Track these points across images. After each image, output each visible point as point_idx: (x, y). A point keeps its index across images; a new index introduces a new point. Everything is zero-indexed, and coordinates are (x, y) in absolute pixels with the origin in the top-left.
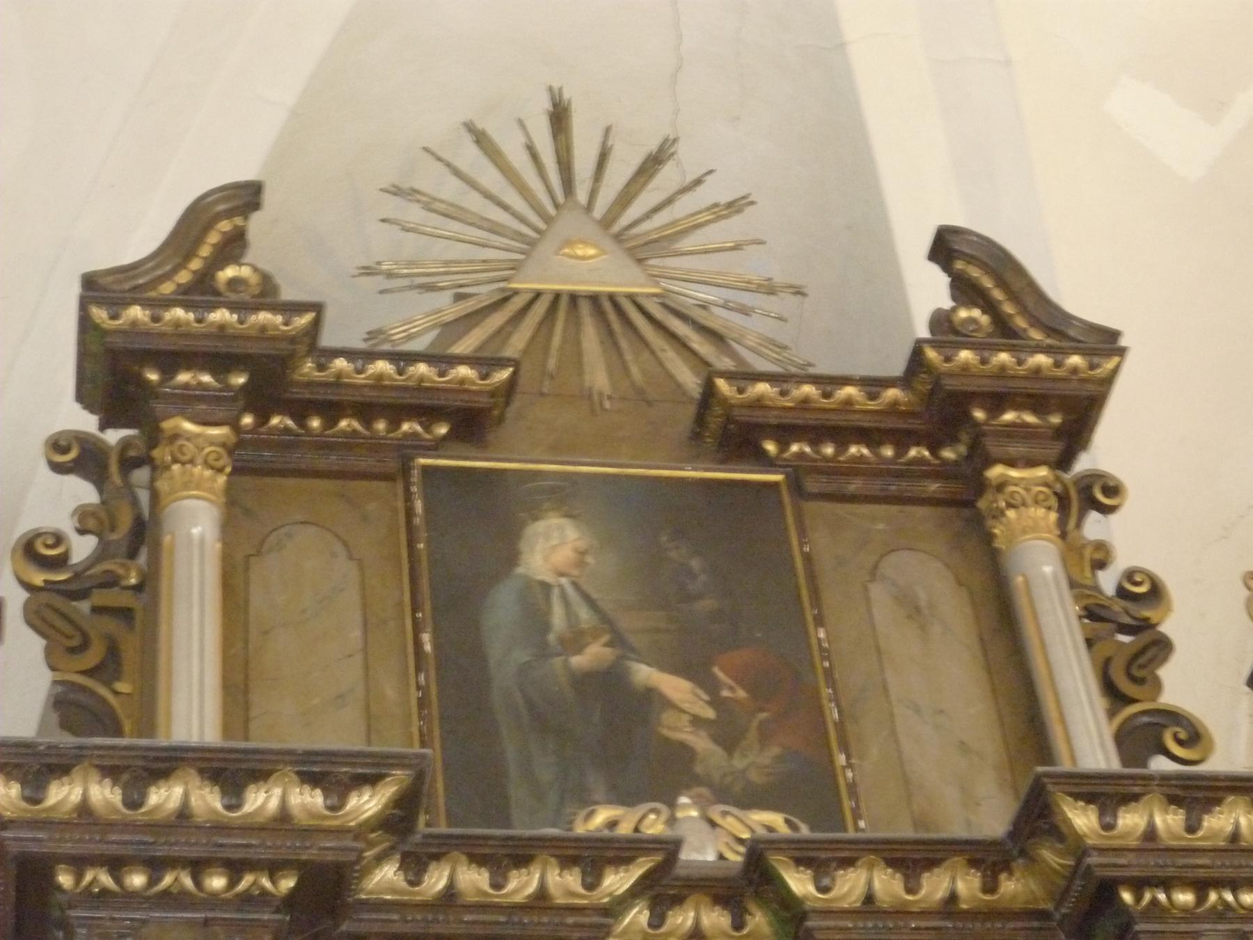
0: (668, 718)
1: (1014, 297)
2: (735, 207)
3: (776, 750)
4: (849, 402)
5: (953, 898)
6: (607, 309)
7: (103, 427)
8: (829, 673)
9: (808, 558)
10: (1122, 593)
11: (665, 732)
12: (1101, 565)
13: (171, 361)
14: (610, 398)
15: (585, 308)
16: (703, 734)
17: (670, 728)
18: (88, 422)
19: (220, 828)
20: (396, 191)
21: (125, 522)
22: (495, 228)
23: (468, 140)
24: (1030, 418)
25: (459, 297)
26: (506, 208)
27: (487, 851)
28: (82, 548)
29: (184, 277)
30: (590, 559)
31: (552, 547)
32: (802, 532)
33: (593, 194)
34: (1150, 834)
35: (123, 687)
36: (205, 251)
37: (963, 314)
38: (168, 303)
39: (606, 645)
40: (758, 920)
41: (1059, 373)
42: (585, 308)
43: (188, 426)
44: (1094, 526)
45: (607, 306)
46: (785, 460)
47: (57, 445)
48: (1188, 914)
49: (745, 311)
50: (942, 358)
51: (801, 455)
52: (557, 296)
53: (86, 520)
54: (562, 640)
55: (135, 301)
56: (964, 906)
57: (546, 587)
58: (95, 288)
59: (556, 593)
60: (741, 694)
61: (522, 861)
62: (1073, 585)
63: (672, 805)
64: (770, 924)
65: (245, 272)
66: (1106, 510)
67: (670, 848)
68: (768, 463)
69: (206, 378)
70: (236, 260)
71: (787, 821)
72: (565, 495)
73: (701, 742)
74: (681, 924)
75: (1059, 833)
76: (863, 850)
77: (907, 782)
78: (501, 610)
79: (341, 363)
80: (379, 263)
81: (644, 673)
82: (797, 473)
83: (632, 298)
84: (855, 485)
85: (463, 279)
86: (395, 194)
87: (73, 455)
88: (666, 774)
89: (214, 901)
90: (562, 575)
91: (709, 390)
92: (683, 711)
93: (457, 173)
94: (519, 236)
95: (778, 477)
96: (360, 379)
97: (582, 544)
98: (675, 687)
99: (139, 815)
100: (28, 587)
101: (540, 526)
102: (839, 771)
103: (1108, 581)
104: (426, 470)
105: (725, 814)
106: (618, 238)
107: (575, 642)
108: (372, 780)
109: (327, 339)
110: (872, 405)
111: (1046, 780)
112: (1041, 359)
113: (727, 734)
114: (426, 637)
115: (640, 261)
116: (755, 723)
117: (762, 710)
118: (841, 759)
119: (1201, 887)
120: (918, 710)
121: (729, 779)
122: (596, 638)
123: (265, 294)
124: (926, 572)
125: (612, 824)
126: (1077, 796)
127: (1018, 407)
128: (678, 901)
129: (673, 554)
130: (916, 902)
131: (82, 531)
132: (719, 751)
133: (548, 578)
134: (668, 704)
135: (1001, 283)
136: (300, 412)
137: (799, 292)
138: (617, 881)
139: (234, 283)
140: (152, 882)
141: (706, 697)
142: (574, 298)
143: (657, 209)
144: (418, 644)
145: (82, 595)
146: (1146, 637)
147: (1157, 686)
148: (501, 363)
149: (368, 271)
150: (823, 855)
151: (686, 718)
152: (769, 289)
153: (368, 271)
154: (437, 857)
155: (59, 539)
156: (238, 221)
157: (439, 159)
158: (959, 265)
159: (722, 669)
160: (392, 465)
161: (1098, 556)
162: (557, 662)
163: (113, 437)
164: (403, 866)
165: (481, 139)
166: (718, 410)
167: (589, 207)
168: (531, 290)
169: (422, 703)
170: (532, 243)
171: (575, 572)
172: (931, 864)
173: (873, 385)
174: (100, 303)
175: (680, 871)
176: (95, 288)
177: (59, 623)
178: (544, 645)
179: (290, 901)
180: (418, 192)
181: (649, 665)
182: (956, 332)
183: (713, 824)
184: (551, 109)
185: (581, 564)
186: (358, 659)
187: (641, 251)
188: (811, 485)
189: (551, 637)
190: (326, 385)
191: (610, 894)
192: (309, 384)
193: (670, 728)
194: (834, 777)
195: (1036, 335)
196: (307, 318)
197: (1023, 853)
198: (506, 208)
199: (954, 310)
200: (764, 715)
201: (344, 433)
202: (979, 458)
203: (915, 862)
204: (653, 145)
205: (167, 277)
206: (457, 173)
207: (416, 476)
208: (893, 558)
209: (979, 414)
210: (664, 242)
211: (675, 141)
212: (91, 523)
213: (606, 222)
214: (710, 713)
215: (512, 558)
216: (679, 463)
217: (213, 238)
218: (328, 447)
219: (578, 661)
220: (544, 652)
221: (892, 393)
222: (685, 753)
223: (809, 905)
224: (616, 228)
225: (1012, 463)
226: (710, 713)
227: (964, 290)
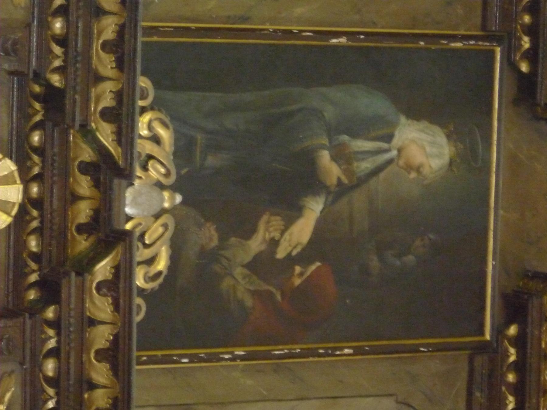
0: (277, 222)
3: (249, 302)
5: (92, 386)
8: (314, 353)
9: (415, 349)
11: (265, 218)
16: (263, 247)
17: (268, 222)
27: (127, 36)
30: (413, 175)
31: (424, 148)
32: (438, 348)
39: (339, 179)
40: (83, 244)
54: (343, 145)
56: (86, 396)
57: (389, 138)
59: (384, 145)
60: (297, 282)
61: (120, 65)
63: (174, 188)
64: (81, 253)
71: (160, 273)
72: (470, 160)
73: (256, 244)
74: (81, 186)
76: (125, 317)
78: (370, 102)
81: (315, 207)
82: (492, 351)
90: (400, 151)
92: (283, 233)
97: (426, 171)
98: (303, 230)
101: (441, 138)
102: (230, 350)
104: (492, 53)
105: (165, 226)
107: (341, 156)
113: (264, 265)
114: (343, 40)
117: (283, 295)
118: (240, 352)
121: (224, 262)
122: (345, 171)
125: (156, 139)
128: (97, 184)
129: (418, 242)
130: (90, 360)
132: (247, 259)
133: (397, 141)
134: (289, 222)
138: (105, 134)
141: (294, 253)
150: (121, 285)
151: (276, 235)
160: (494, 26)
162: (325, 141)
169: (288, 34)
171: (401, 163)
172: (115, 369)
178: (340, 132)
181: (322, 212)
183: (157, 217)
185: (409, 168)
188: (480, 361)
193: (268, 222)
200: (279, 297)
203: (115, 357)
207: (485, 45)
214: (281, 254)
215: (414, 114)
216: (500, 254)
219: (325, 157)
220: (332, 131)
222: (249, 233)
223: (88, 277)
226: (281, 254)
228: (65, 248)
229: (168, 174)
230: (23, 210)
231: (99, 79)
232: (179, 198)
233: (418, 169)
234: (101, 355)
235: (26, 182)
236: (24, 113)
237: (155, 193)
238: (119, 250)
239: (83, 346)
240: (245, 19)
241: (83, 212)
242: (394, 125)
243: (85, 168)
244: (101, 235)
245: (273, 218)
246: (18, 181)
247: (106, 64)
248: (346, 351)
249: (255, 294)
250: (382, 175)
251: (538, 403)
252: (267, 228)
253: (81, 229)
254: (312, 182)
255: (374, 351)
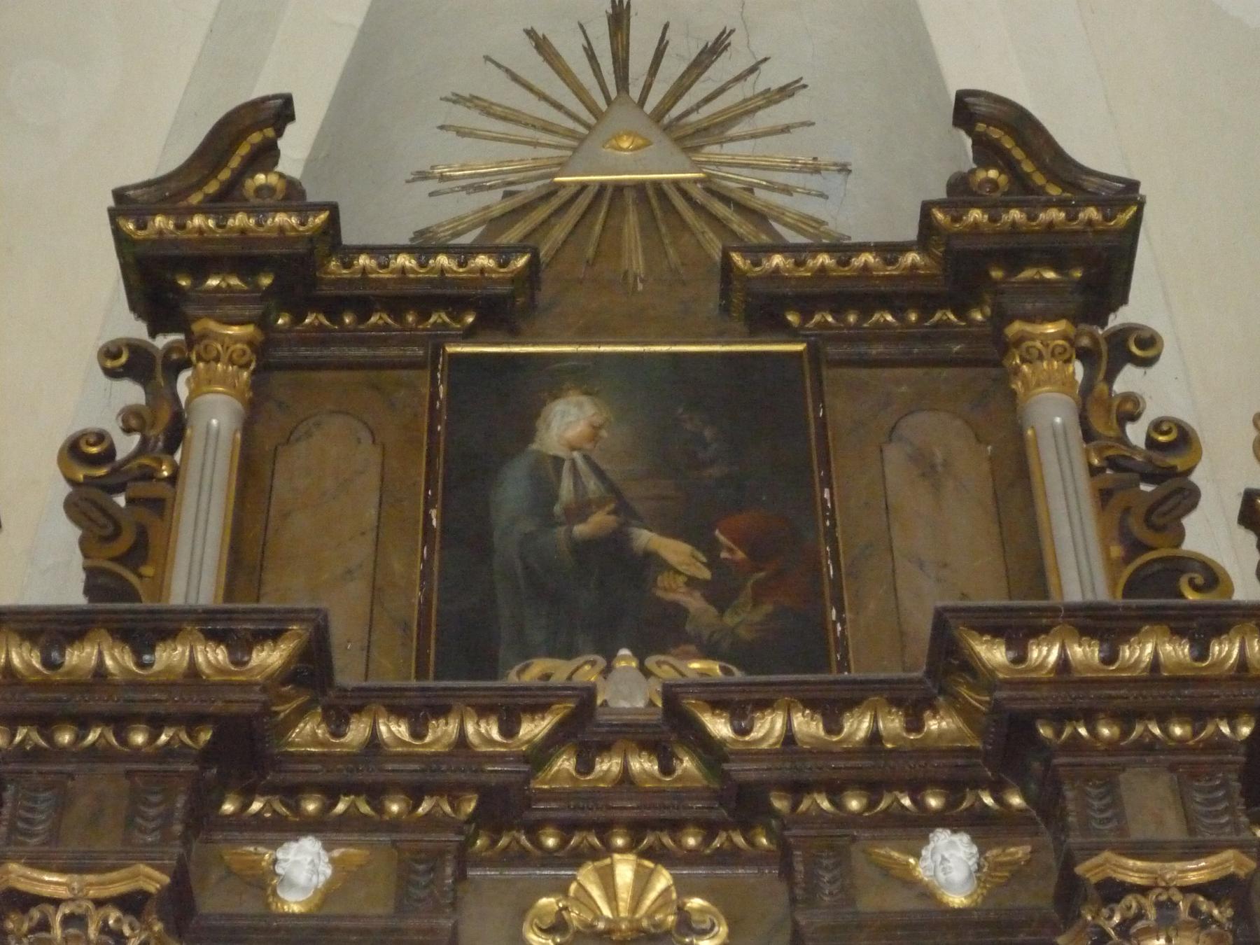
0: (664, 580)
1: (1031, 155)
2: (786, 92)
3: (767, 608)
4: (866, 267)
6: (653, 198)
7: (153, 334)
10: (1151, 443)
11: (660, 593)
12: (1134, 418)
13: (202, 265)
14: (642, 281)
15: (630, 196)
16: (697, 594)
17: (665, 590)
18: (137, 330)
19: (135, 684)
20: (457, 99)
21: (165, 416)
22: (547, 128)
23: (528, 46)
24: (1050, 275)
25: (508, 195)
26: (558, 107)
27: (404, 702)
28: (126, 445)
29: (212, 188)
30: (604, 433)
31: (567, 422)
33: (647, 88)
34: (1064, 664)
35: (148, 570)
36: (235, 162)
37: (981, 175)
38: (192, 211)
39: (609, 513)
40: (687, 764)
41: (1074, 225)
42: (630, 196)
43: (212, 325)
44: (1128, 380)
45: (651, 192)
46: (809, 329)
47: (109, 352)
48: (1112, 747)
49: (787, 190)
50: (949, 218)
51: (824, 325)
52: (603, 186)
53: (132, 420)
54: (567, 510)
55: (166, 213)
56: (889, 746)
57: (558, 461)
58: (125, 204)
59: (567, 465)
60: (740, 555)
61: (441, 711)
62: (1088, 435)
63: (610, 656)
64: (698, 768)
65: (273, 179)
66: (1147, 363)
67: (588, 693)
68: (792, 334)
69: (234, 281)
70: (267, 170)
71: (723, 669)
72: (583, 374)
73: (694, 602)
74: (609, 770)
75: (971, 668)
76: (780, 691)
77: (902, 634)
79: (363, 260)
80: (433, 167)
81: (645, 538)
83: (676, 183)
84: (876, 350)
85: (512, 178)
86: (454, 102)
87: (124, 359)
88: (659, 631)
89: (137, 754)
90: (573, 449)
91: (727, 264)
92: (678, 572)
93: (515, 78)
94: (571, 134)
95: (799, 347)
96: (384, 274)
97: (598, 420)
98: (675, 551)
99: (57, 677)
100: (72, 482)
102: (830, 627)
103: (1136, 433)
105: (659, 664)
106: (667, 129)
107: (581, 511)
108: (275, 636)
109: (350, 235)
110: (891, 271)
111: (947, 615)
112: (1056, 215)
113: (720, 592)
115: (686, 150)
116: (750, 583)
119: (1126, 718)
120: (921, 565)
121: (716, 636)
123: (292, 196)
124: (941, 431)
126: (982, 631)
127: (1039, 264)
128: (605, 748)
129: (689, 426)
130: (840, 742)
131: (128, 430)
132: (713, 610)
133: (562, 452)
134: (665, 566)
135: (1022, 143)
136: (333, 307)
137: (844, 169)
138: (533, 729)
139: (260, 190)
140: (80, 737)
141: (704, 560)
142: (619, 188)
143: (708, 100)
144: (427, 518)
145: (119, 489)
146: (1171, 484)
147: (1180, 534)
148: (519, 249)
149: (423, 176)
150: (737, 697)
151: (681, 580)
152: (815, 169)
153: (423, 176)
154: (358, 710)
155: (101, 437)
156: (270, 132)
157: (499, 66)
158: (981, 127)
159: (722, 532)
161: (1129, 406)
162: (562, 530)
163: (161, 342)
164: (326, 718)
165: (542, 45)
166: (736, 284)
167: (642, 102)
168: (576, 183)
169: (425, 575)
170: (582, 139)
171: (588, 446)
173: (888, 251)
174: (127, 215)
175: (602, 718)
176: (125, 204)
177: (96, 514)
178: (551, 515)
179: (207, 756)
180: (477, 98)
181: (651, 531)
182: (975, 194)
183: (647, 673)
184: (610, 11)
186: (371, 536)
187: (689, 139)
189: (557, 509)
190: (350, 282)
191: (528, 742)
192: (339, 282)
193: (665, 590)
194: (825, 629)
195: (1054, 191)
196: (323, 216)
197: (942, 691)
198: (558, 107)
199: (972, 172)
200: (762, 574)
201: (376, 327)
202: (1001, 318)
203: (834, 702)
204: (711, 37)
205: (198, 186)
206: (515, 78)
208: (913, 420)
209: (997, 274)
210: (716, 129)
211: (732, 31)
212: (134, 423)
213: (658, 114)
214: (706, 574)
215: (527, 433)
217: (244, 150)
218: (361, 342)
219: (581, 530)
220: (549, 521)
221: (912, 257)
222: (678, 613)
224: (666, 120)
225: (1029, 318)
226: (706, 574)
227: (986, 152)
228: (695, 790)
229: (593, 663)
230: (647, 854)
231: (462, 739)
232: (624, 652)
233: (596, 429)
234: (833, 726)
235: (609, 850)
236: (519, 858)
237: (614, 676)
238: (690, 703)
239: (820, 752)
240: (406, 627)
241: (644, 765)
242: (541, 458)
243: (585, 766)
244: (673, 737)
245: (659, 584)
246: (608, 861)
247: (442, 732)
248: (827, 495)
249: (756, 601)
250: (604, 466)
251: (878, 277)
252: (672, 591)
253: (666, 769)
254: (615, 543)
255: (826, 462)
